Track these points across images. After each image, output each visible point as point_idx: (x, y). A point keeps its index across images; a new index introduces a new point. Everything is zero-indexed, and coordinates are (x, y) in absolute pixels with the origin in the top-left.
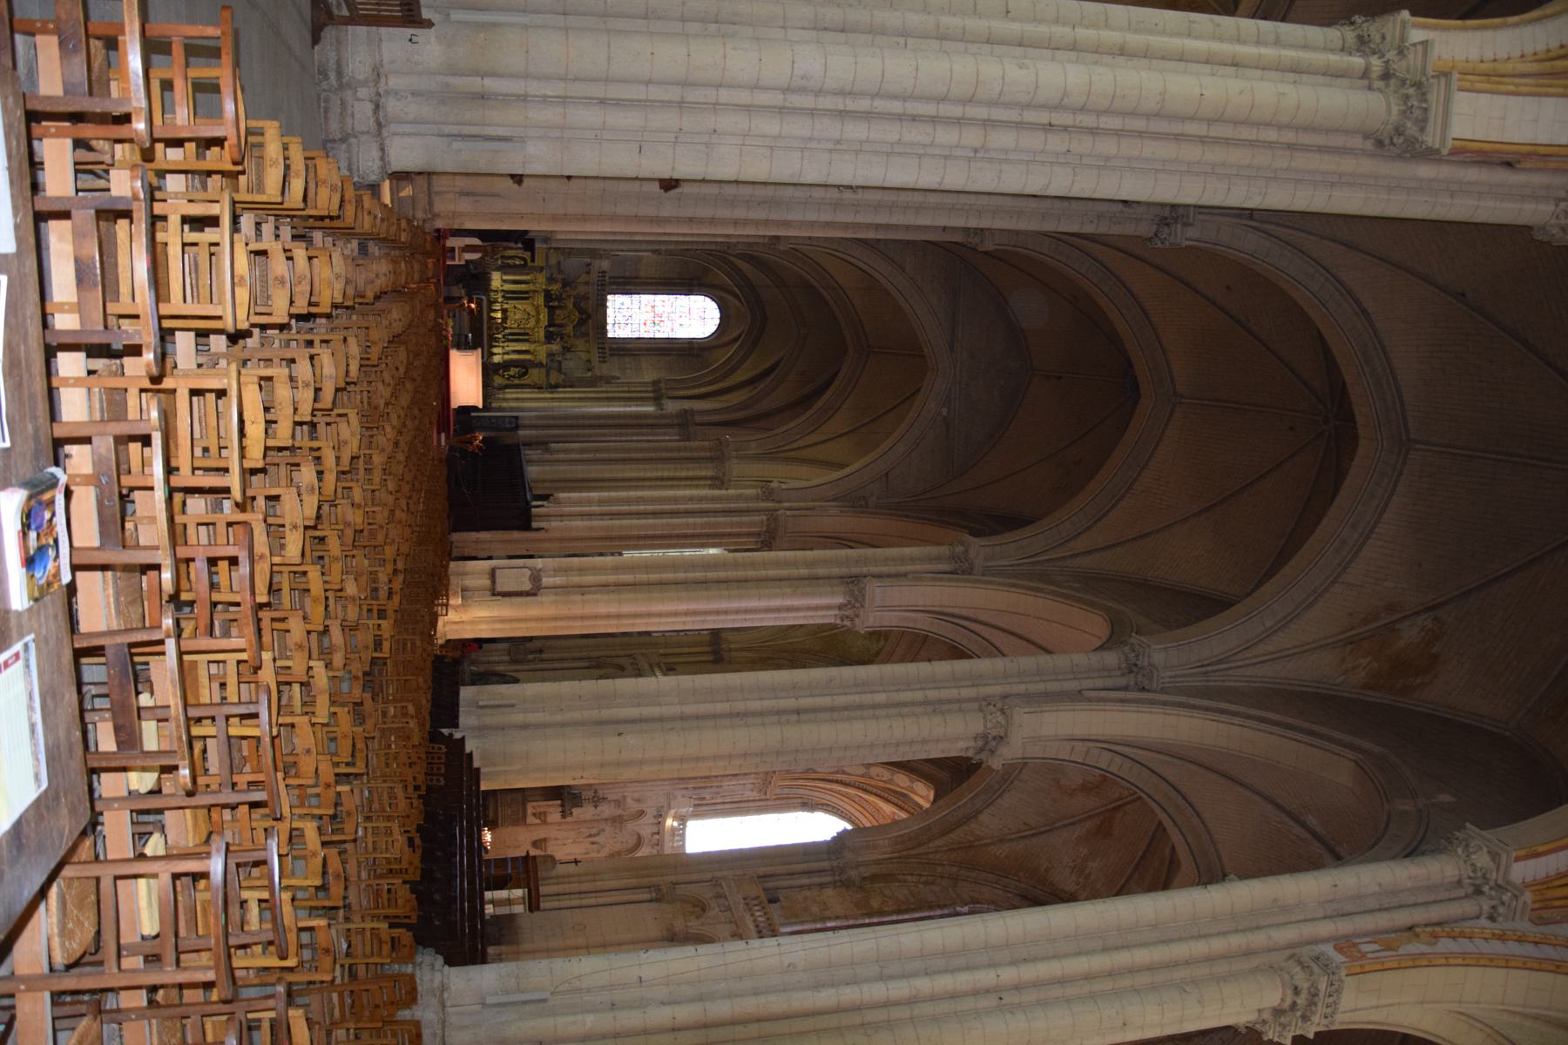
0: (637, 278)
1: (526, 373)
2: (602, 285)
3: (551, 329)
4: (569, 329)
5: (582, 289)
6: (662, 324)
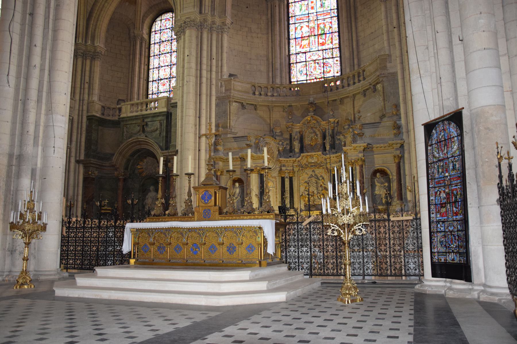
0: (268, 60)
1: (383, 173)
5: (278, 115)
6: (322, 26)
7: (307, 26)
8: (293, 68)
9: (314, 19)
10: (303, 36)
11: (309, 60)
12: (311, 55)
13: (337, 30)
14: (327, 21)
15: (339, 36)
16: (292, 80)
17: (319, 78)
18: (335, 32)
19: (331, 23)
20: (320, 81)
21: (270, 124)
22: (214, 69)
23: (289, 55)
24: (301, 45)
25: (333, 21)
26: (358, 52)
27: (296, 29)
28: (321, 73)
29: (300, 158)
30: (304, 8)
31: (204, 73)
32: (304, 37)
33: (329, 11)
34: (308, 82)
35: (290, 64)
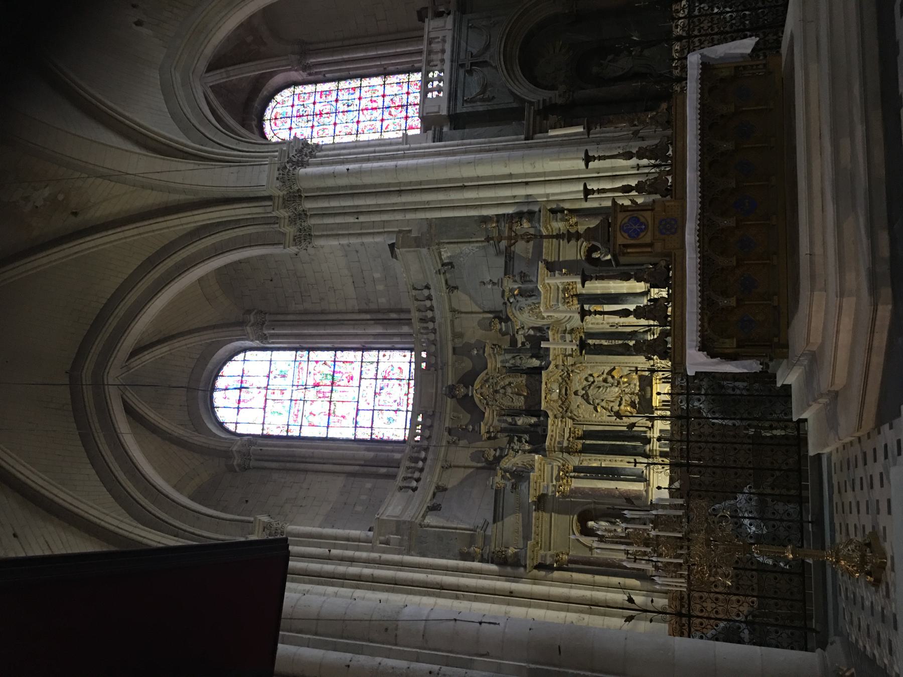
2: (415, 460)
3: (536, 363)
4: (495, 362)
5: (462, 455)
7: (311, 404)
8: (380, 436)
10: (327, 412)
12: (364, 399)
13: (332, 353)
15: (343, 349)
16: (401, 438)
17: (409, 388)
18: (335, 355)
19: (317, 362)
21: (478, 468)
22: (349, 553)
23: (356, 441)
26: (378, 311)
27: (311, 425)
29: (550, 413)
30: (278, 407)
31: (354, 570)
32: (330, 410)
34: (410, 408)
35: (372, 441)
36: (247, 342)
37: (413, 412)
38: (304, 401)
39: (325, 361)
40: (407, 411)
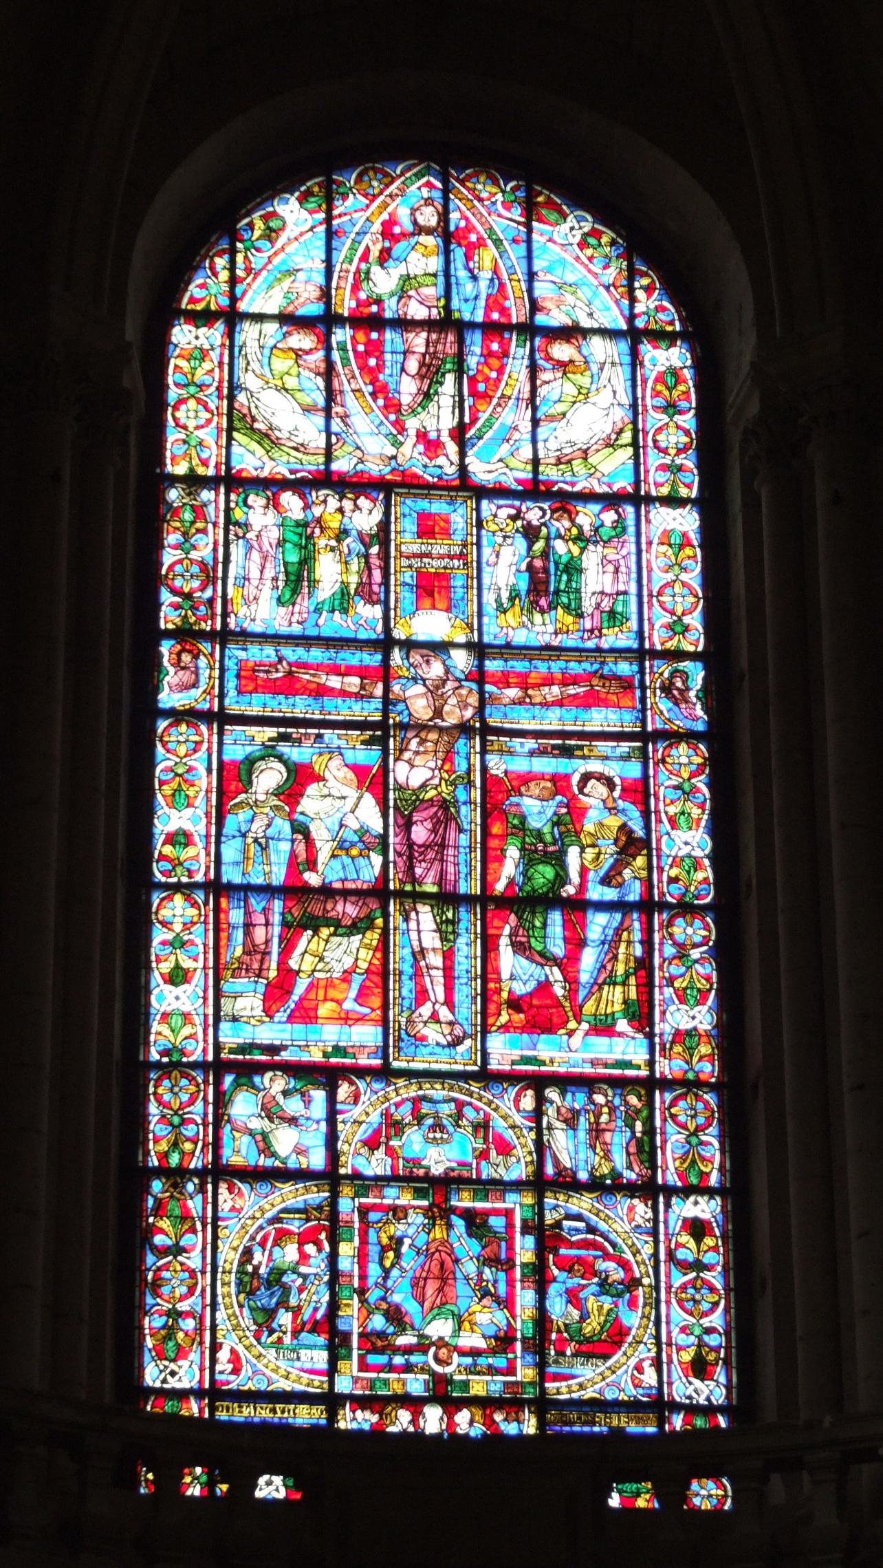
7: (360, 771)
9: (452, 718)
11: (377, 1165)
12: (405, 1112)
14: (594, 766)
17: (486, 1404)
18: (685, 909)
19: (639, 792)
20: (495, 1439)
24: (287, 976)
25: (664, 782)
28: (504, 1341)
32: (326, 891)
33: (625, 668)
36: (752, 339)
37: (326, 1434)
38: (383, 725)
39: (646, 843)
40: (332, 1401)
